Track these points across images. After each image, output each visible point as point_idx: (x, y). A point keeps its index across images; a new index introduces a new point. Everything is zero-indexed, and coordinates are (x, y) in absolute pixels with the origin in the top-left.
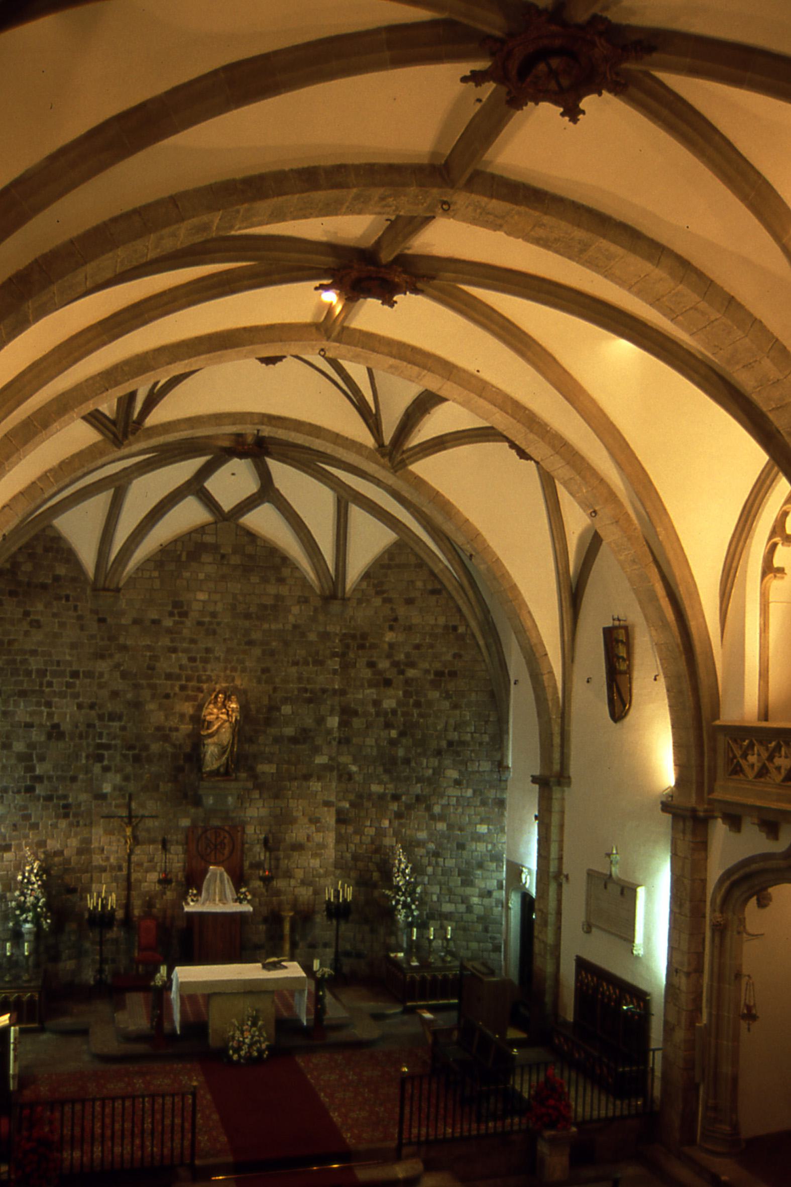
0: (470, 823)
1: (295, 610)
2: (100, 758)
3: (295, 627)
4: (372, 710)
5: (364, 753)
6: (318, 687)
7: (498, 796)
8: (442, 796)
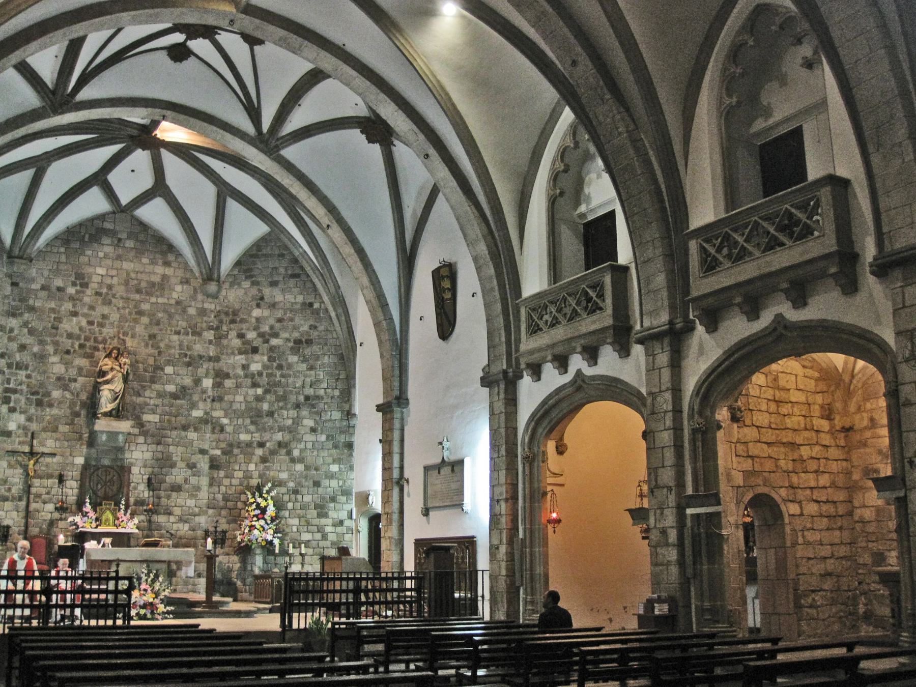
0: (324, 464)
1: (179, 288)
3: (178, 303)
4: (241, 373)
5: (234, 408)
6: (196, 354)
7: (347, 439)
8: (300, 441)
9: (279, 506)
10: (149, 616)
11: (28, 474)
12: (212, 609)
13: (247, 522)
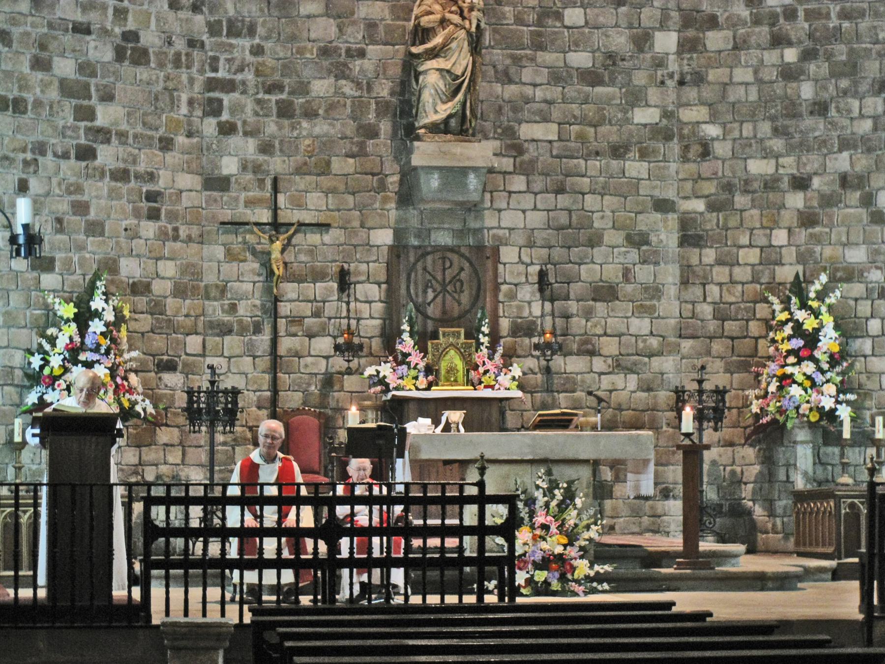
2: (213, 108)
5: (732, 99)
9: (848, 328)
10: (556, 585)
11: (271, 273)
12: (701, 570)
13: (773, 368)
